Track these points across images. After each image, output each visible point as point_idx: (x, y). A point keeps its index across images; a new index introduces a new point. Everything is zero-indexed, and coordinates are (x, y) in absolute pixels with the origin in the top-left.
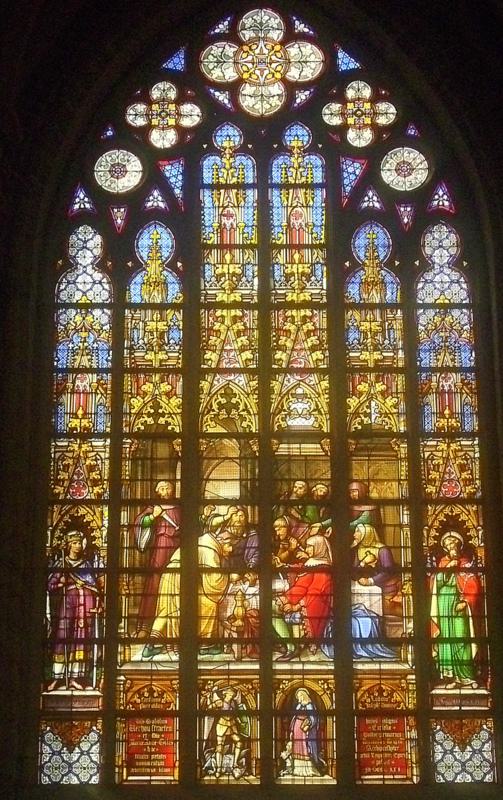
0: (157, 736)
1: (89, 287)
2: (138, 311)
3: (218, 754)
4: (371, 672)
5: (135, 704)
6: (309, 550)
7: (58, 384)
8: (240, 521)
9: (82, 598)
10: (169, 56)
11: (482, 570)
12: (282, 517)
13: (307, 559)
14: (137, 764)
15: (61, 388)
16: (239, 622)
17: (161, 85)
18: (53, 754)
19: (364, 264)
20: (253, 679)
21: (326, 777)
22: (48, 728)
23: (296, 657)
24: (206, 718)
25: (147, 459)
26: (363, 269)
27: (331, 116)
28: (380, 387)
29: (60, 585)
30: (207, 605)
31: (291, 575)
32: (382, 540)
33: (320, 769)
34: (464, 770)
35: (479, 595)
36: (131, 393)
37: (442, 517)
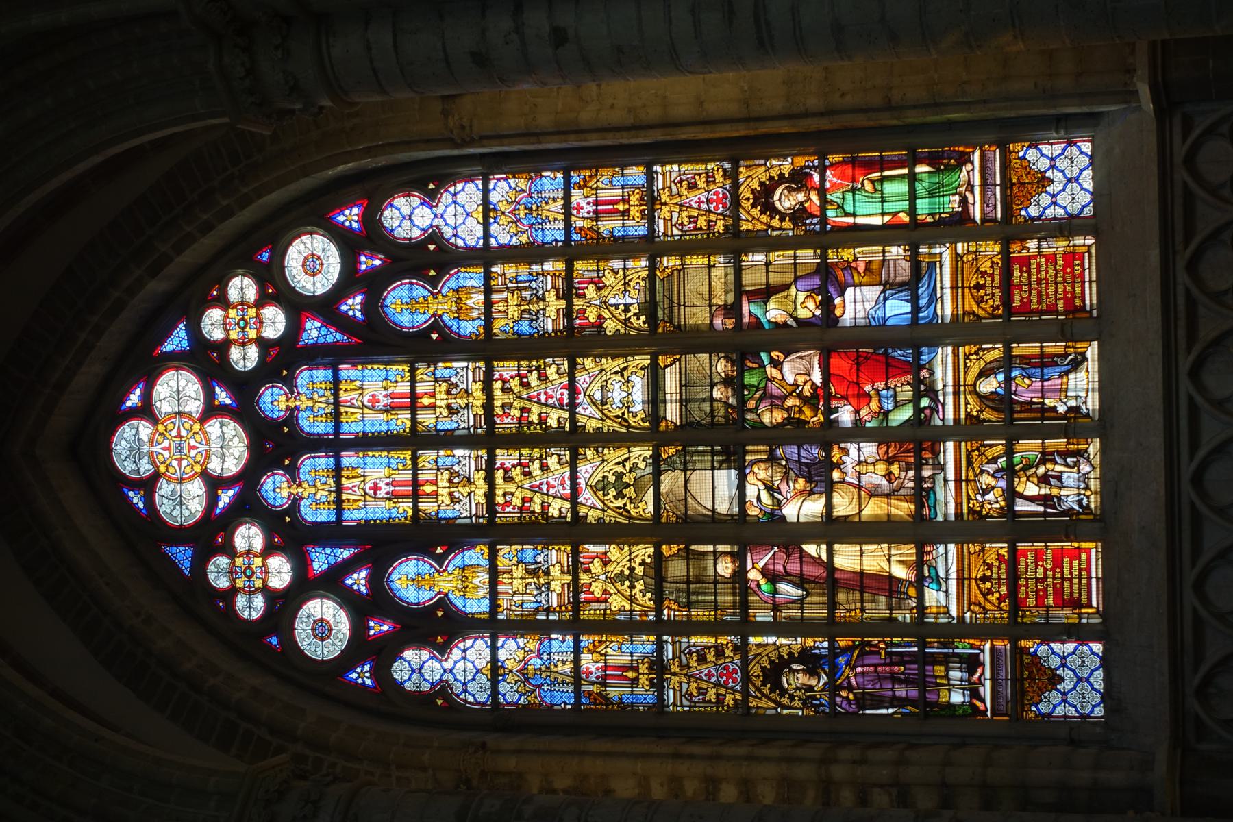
0: (1041, 570)
1: (470, 666)
2: (499, 602)
3: (1063, 493)
4: (955, 298)
5: (1001, 599)
6: (800, 380)
7: (595, 704)
8: (766, 469)
9: (867, 669)
10: (173, 565)
11: (823, 157)
12: (759, 416)
13: (813, 384)
14: (1076, 594)
15: (600, 700)
16: (895, 469)
17: (212, 577)
18: (1065, 701)
19: (434, 315)
20: (967, 450)
21: (1088, 355)
22: (1033, 708)
23: (937, 396)
24: (1017, 508)
25: (688, 588)
26: (440, 316)
27: (245, 359)
28: (591, 292)
29: (851, 697)
30: (874, 509)
31: (834, 404)
32: (786, 287)
33: (1078, 363)
34: (1077, 180)
35: (854, 163)
36: (605, 610)
37: (756, 212)
